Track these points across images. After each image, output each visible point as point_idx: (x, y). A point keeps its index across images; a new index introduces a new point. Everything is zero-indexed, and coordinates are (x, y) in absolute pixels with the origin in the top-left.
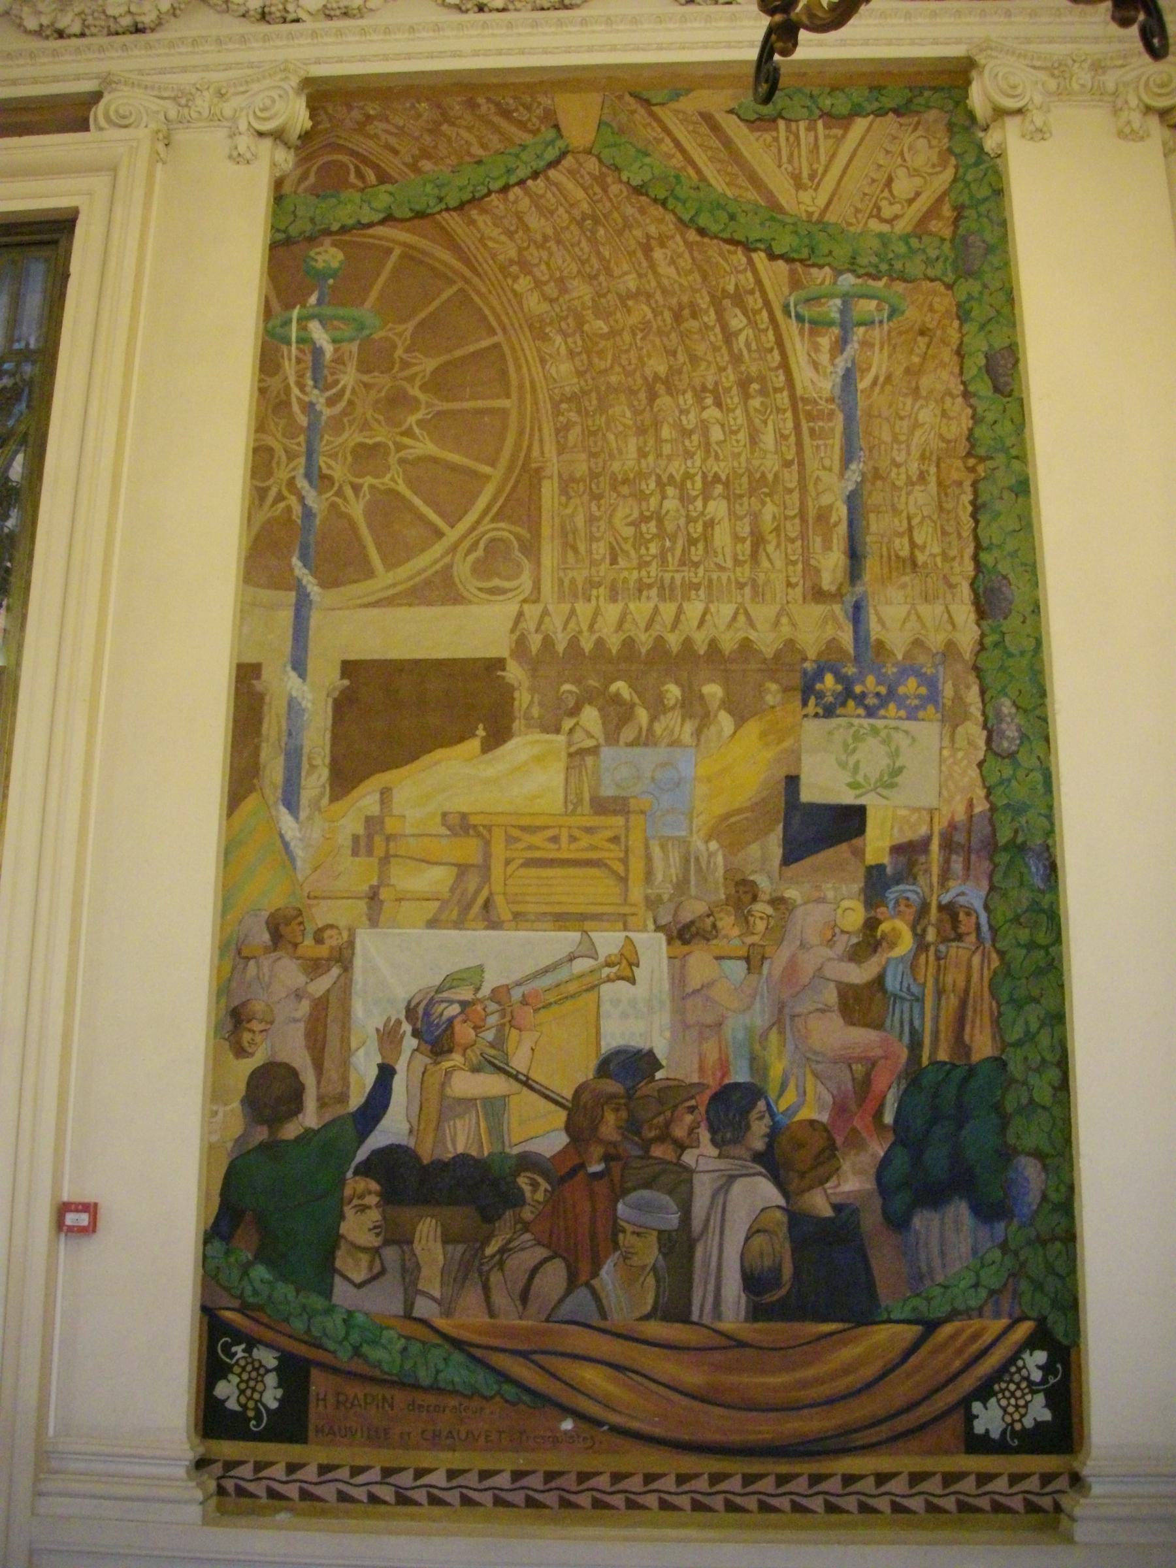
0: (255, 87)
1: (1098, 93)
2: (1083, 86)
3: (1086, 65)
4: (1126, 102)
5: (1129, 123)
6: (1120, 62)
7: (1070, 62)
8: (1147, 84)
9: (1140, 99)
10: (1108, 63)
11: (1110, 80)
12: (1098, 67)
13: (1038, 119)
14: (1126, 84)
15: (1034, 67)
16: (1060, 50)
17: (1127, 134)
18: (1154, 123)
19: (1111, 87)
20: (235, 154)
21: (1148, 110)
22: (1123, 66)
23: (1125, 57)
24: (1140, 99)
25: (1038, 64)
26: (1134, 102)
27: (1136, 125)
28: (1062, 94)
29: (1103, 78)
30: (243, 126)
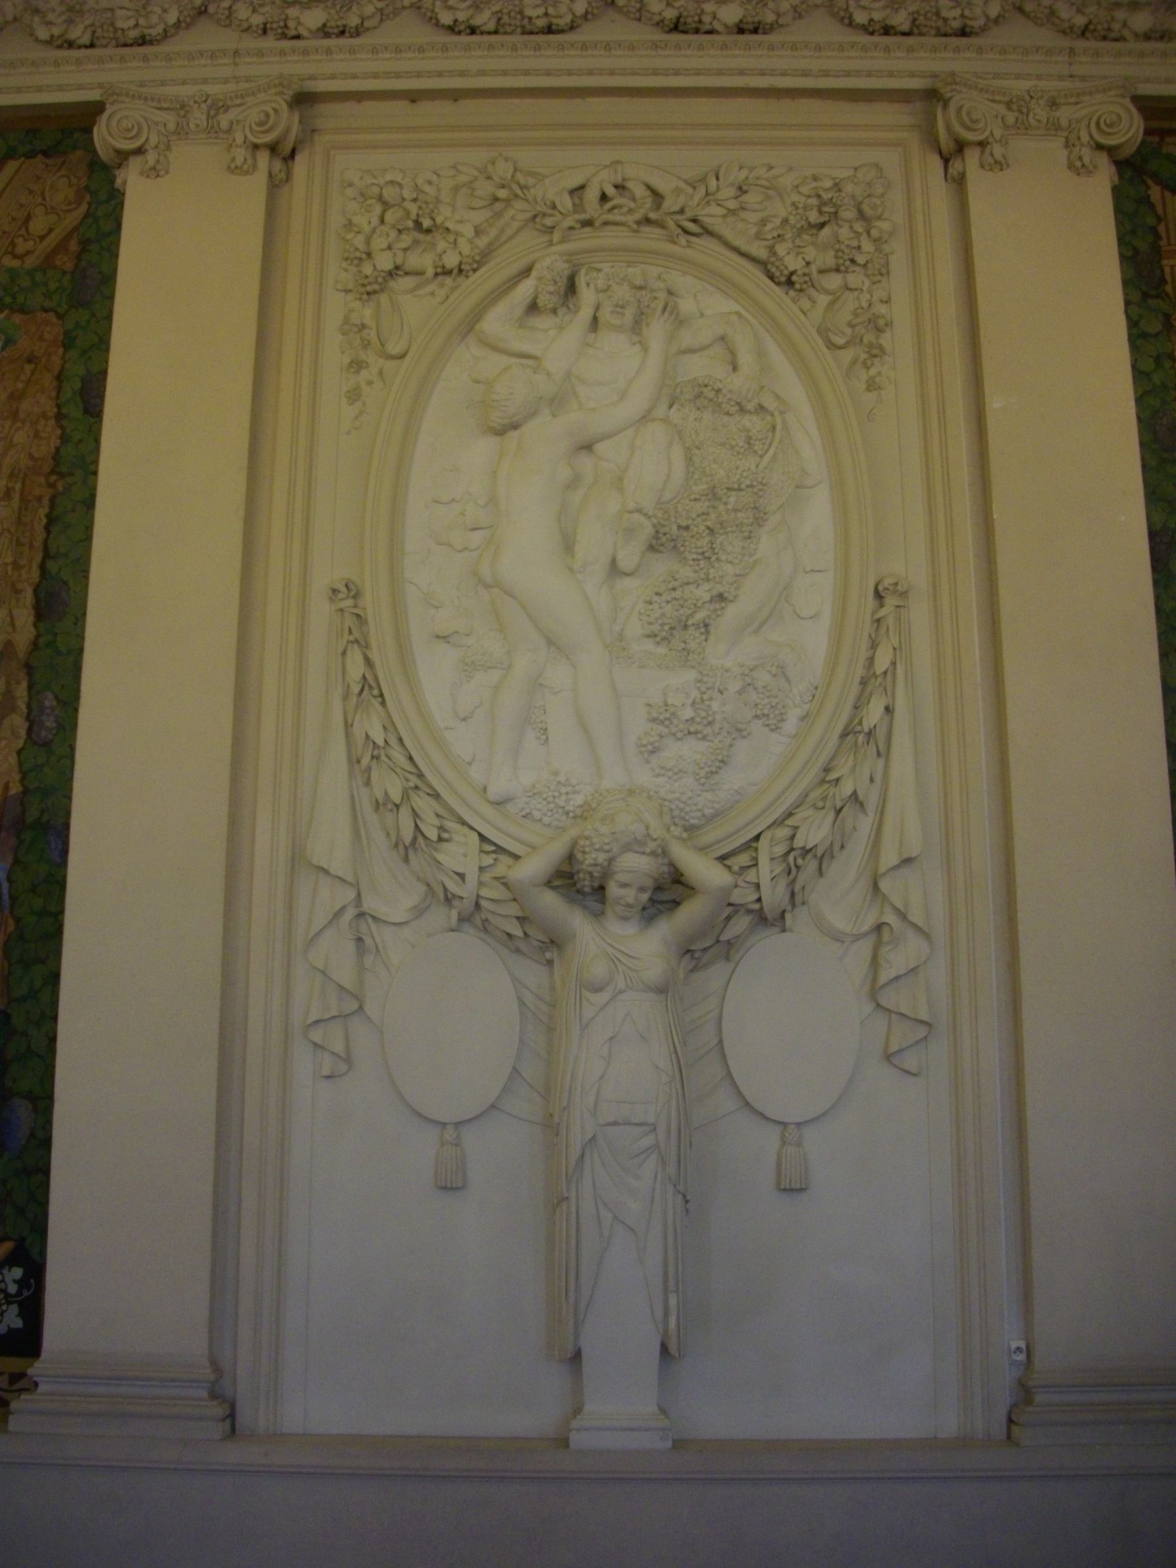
0: (250, 100)
1: (1054, 127)
2: (1039, 121)
3: (1042, 102)
4: (1079, 138)
5: (1080, 158)
6: (1072, 100)
7: (1027, 98)
8: (1098, 123)
9: (1091, 136)
10: (1062, 101)
11: (1065, 114)
12: (1053, 104)
13: (998, 151)
14: (1078, 121)
15: (993, 101)
16: (1020, 86)
17: (1078, 168)
18: (1103, 159)
19: (1064, 123)
20: (233, 166)
21: (1099, 147)
22: (1077, 103)
23: (1078, 95)
24: (1091, 136)
25: (998, 98)
26: (1085, 138)
27: (1086, 160)
28: (1022, 127)
29: (1058, 114)
30: (239, 139)
